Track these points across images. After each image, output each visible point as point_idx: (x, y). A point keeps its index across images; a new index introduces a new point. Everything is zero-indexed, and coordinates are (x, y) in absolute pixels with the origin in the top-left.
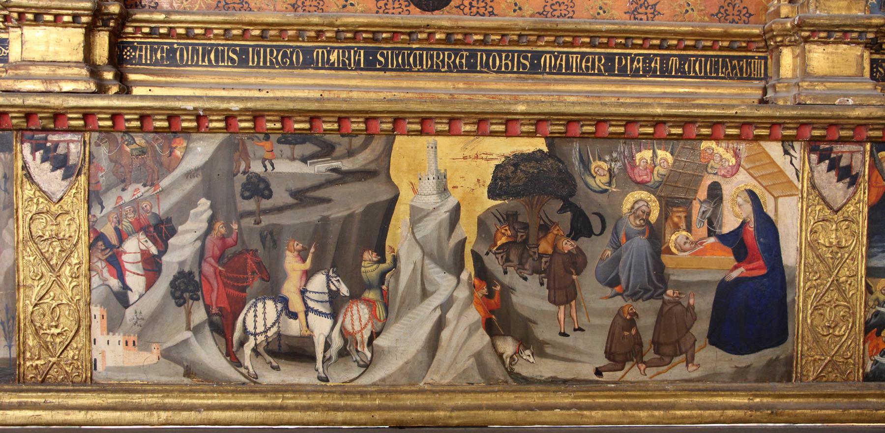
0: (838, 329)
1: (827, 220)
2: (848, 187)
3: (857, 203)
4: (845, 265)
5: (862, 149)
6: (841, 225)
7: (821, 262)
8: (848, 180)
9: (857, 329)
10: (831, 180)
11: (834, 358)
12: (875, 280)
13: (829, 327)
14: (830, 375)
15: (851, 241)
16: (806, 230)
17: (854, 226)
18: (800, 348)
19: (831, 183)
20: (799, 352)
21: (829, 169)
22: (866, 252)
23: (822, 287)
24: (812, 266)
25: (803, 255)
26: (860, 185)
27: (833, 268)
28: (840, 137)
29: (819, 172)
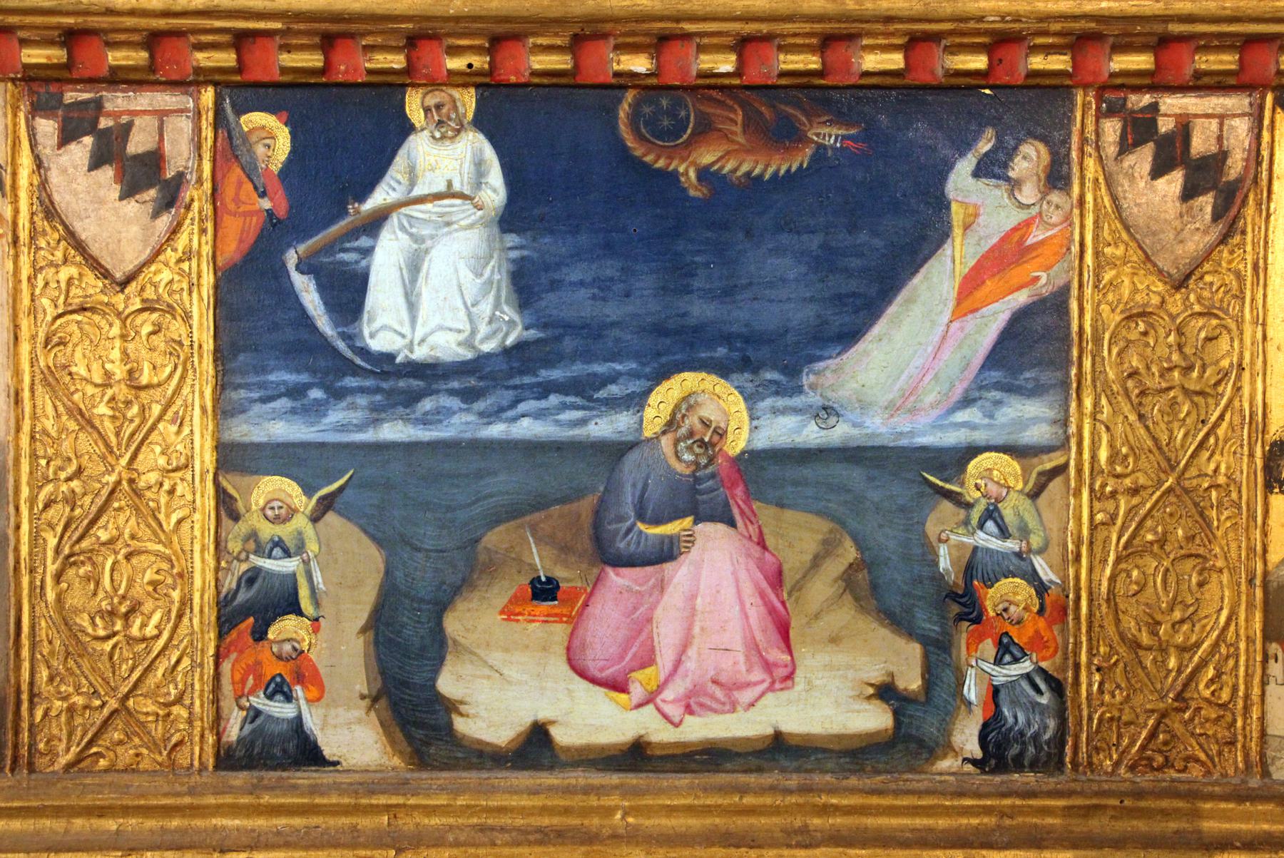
0: (138, 622)
1: (93, 310)
2: (156, 215)
3: (180, 261)
4: (154, 437)
5: (191, 105)
6: (139, 320)
7: (82, 428)
8: (153, 193)
9: (196, 621)
10: (102, 193)
11: (131, 703)
12: (247, 480)
13: (112, 613)
14: (120, 750)
15: (168, 370)
16: (34, 337)
17: (176, 328)
18: (25, 675)
19: (102, 202)
20: (25, 687)
21: (97, 162)
22: (216, 401)
23: (88, 500)
24: (56, 441)
25: (28, 409)
26: (188, 208)
27: (119, 444)
28: (115, 70)
29: (64, 171)
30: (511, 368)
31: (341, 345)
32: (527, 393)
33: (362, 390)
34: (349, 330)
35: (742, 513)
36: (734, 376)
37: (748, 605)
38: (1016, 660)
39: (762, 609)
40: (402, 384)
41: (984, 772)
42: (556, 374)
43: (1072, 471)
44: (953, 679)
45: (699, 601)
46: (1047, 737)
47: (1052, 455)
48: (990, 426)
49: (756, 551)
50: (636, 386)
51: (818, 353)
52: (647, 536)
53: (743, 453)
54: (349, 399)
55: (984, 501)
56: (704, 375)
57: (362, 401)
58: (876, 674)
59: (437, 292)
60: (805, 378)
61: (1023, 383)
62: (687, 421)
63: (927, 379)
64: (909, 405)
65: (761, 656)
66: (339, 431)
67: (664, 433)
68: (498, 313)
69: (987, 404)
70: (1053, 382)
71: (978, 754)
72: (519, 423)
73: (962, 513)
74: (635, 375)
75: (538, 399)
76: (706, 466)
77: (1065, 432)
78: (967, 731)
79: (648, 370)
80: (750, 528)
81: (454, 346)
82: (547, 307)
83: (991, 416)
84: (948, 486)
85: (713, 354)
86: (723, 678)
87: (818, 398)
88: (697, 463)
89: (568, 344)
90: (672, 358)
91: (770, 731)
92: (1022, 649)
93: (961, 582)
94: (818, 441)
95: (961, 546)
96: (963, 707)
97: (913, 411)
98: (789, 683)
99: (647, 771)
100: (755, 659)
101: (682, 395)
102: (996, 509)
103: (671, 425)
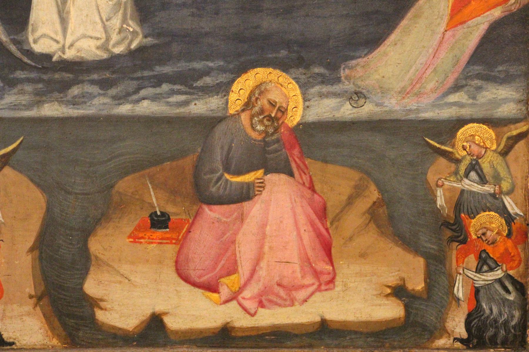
30: (135, 65)
31: (13, 48)
32: (146, 83)
33: (29, 80)
34: (18, 37)
35: (298, 167)
36: (292, 70)
37: (302, 231)
38: (491, 269)
39: (312, 234)
40: (57, 76)
41: (469, 348)
42: (167, 69)
44: (446, 282)
45: (268, 228)
46: (513, 323)
47: (518, 125)
48: (472, 105)
49: (308, 193)
50: (222, 78)
51: (352, 54)
52: (231, 182)
53: (299, 124)
54: (19, 87)
55: (468, 158)
56: (271, 70)
57: (29, 88)
58: (392, 278)
59: (81, 10)
60: (342, 71)
61: (497, 74)
62: (259, 103)
64: (415, 90)
65: (312, 267)
66: (12, 109)
67: (243, 110)
68: (125, 26)
70: (519, 73)
71: (464, 335)
72: (140, 104)
73: (453, 167)
74: (223, 70)
75: (154, 87)
76: (272, 134)
78: (457, 319)
79: (231, 66)
80: (304, 177)
81: (94, 49)
82: (160, 22)
83: (474, 98)
84: (443, 147)
85: (277, 55)
86: (285, 282)
87: (352, 85)
88: (266, 132)
89: (175, 48)
90: (249, 58)
91: (318, 319)
92: (496, 262)
93: (452, 215)
94: (352, 116)
95: (452, 189)
96: (454, 302)
97: (419, 95)
98: (331, 285)
99: (231, 347)
100: (307, 269)
102: (477, 163)
103: (248, 105)
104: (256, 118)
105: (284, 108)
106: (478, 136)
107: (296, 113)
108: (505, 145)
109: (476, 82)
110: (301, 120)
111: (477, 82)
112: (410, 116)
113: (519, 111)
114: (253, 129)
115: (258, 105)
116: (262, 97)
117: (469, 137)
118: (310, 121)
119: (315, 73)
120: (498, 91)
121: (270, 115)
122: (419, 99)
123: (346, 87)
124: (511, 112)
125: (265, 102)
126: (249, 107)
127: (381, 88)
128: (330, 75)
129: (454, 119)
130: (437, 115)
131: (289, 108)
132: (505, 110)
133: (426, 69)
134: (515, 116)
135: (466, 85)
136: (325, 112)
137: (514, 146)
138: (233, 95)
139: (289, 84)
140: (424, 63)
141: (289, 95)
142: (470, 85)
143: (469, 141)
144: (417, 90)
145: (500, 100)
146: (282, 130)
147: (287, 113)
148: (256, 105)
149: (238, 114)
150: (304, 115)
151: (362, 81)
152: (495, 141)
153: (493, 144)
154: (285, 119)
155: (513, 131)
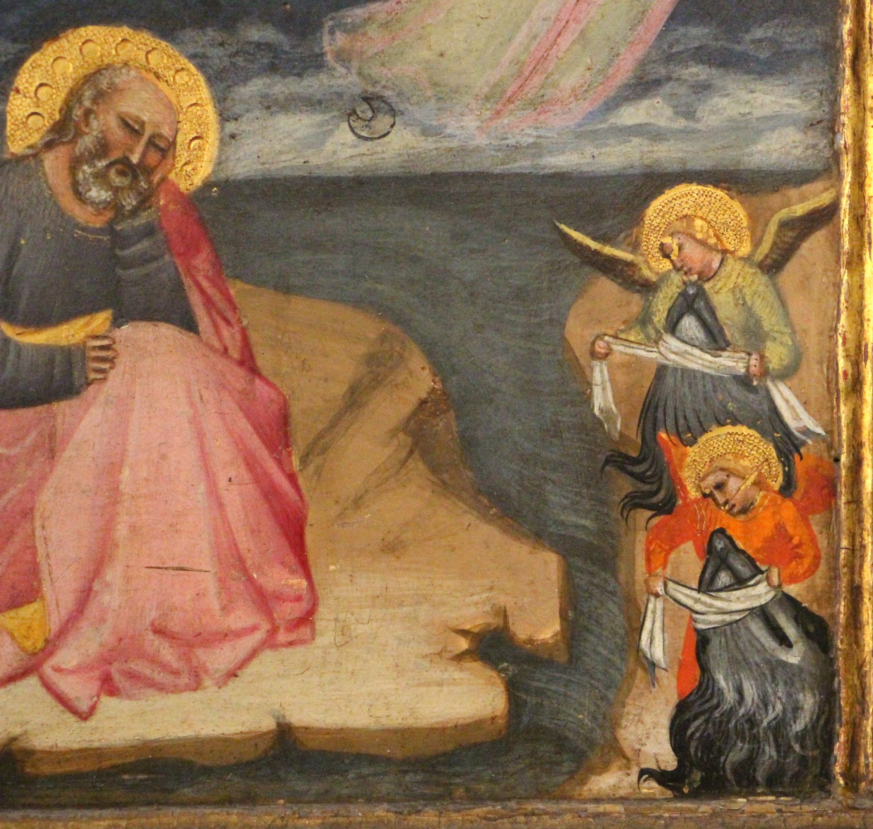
35: (209, 302)
36: (189, 34)
37: (223, 483)
38: (740, 582)
39: (251, 490)
41: (680, 796)
43: (845, 220)
44: (620, 619)
45: (126, 473)
46: (798, 726)
48: (686, 134)
49: (237, 377)
52: (19, 348)
53: (208, 185)
55: (677, 279)
56: (125, 31)
58: (473, 610)
60: (326, 38)
61: (751, 49)
62: (94, 124)
63: (565, 42)
64: (530, 91)
65: (250, 579)
67: (49, 145)
69: (683, 90)
70: (809, 47)
71: (669, 761)
73: (636, 301)
76: (134, 212)
77: (832, 143)
78: (648, 718)
80: (226, 332)
83: (690, 114)
84: (608, 250)
86: (175, 625)
87: (353, 78)
88: (115, 206)
91: (268, 724)
92: (751, 561)
93: (633, 433)
94: (356, 163)
95: (633, 365)
96: (640, 673)
97: (539, 104)
98: (304, 631)
99: (24, 806)
100: (238, 586)
101: (82, 72)
102: (701, 293)
104: (85, 167)
105: (167, 139)
106: (702, 218)
107: (200, 153)
108: (775, 243)
109: (694, 70)
110: (213, 171)
111: (697, 71)
112: (517, 164)
113: (810, 152)
114: (79, 195)
115: (92, 130)
116: (101, 107)
117: (678, 223)
118: (240, 177)
119: (251, 43)
120: (754, 95)
121: (128, 159)
122: (542, 118)
123: (340, 81)
124: (788, 153)
125: (113, 122)
126: (66, 135)
127: (436, 84)
128: (293, 47)
129: (636, 172)
130: (590, 160)
131: (180, 139)
132: (773, 147)
133: (559, 35)
134: (801, 163)
135: (669, 79)
136: (281, 153)
137: (799, 246)
138: (19, 102)
139: (177, 71)
140: (553, 17)
141: (179, 102)
142: (678, 79)
143: (679, 232)
144: (533, 91)
145: (758, 119)
146: (162, 202)
147: (175, 148)
148: (87, 130)
149: (35, 156)
150: (223, 158)
151: (383, 65)
152: (748, 233)
153: (741, 242)
154: (170, 171)
155: (795, 204)
